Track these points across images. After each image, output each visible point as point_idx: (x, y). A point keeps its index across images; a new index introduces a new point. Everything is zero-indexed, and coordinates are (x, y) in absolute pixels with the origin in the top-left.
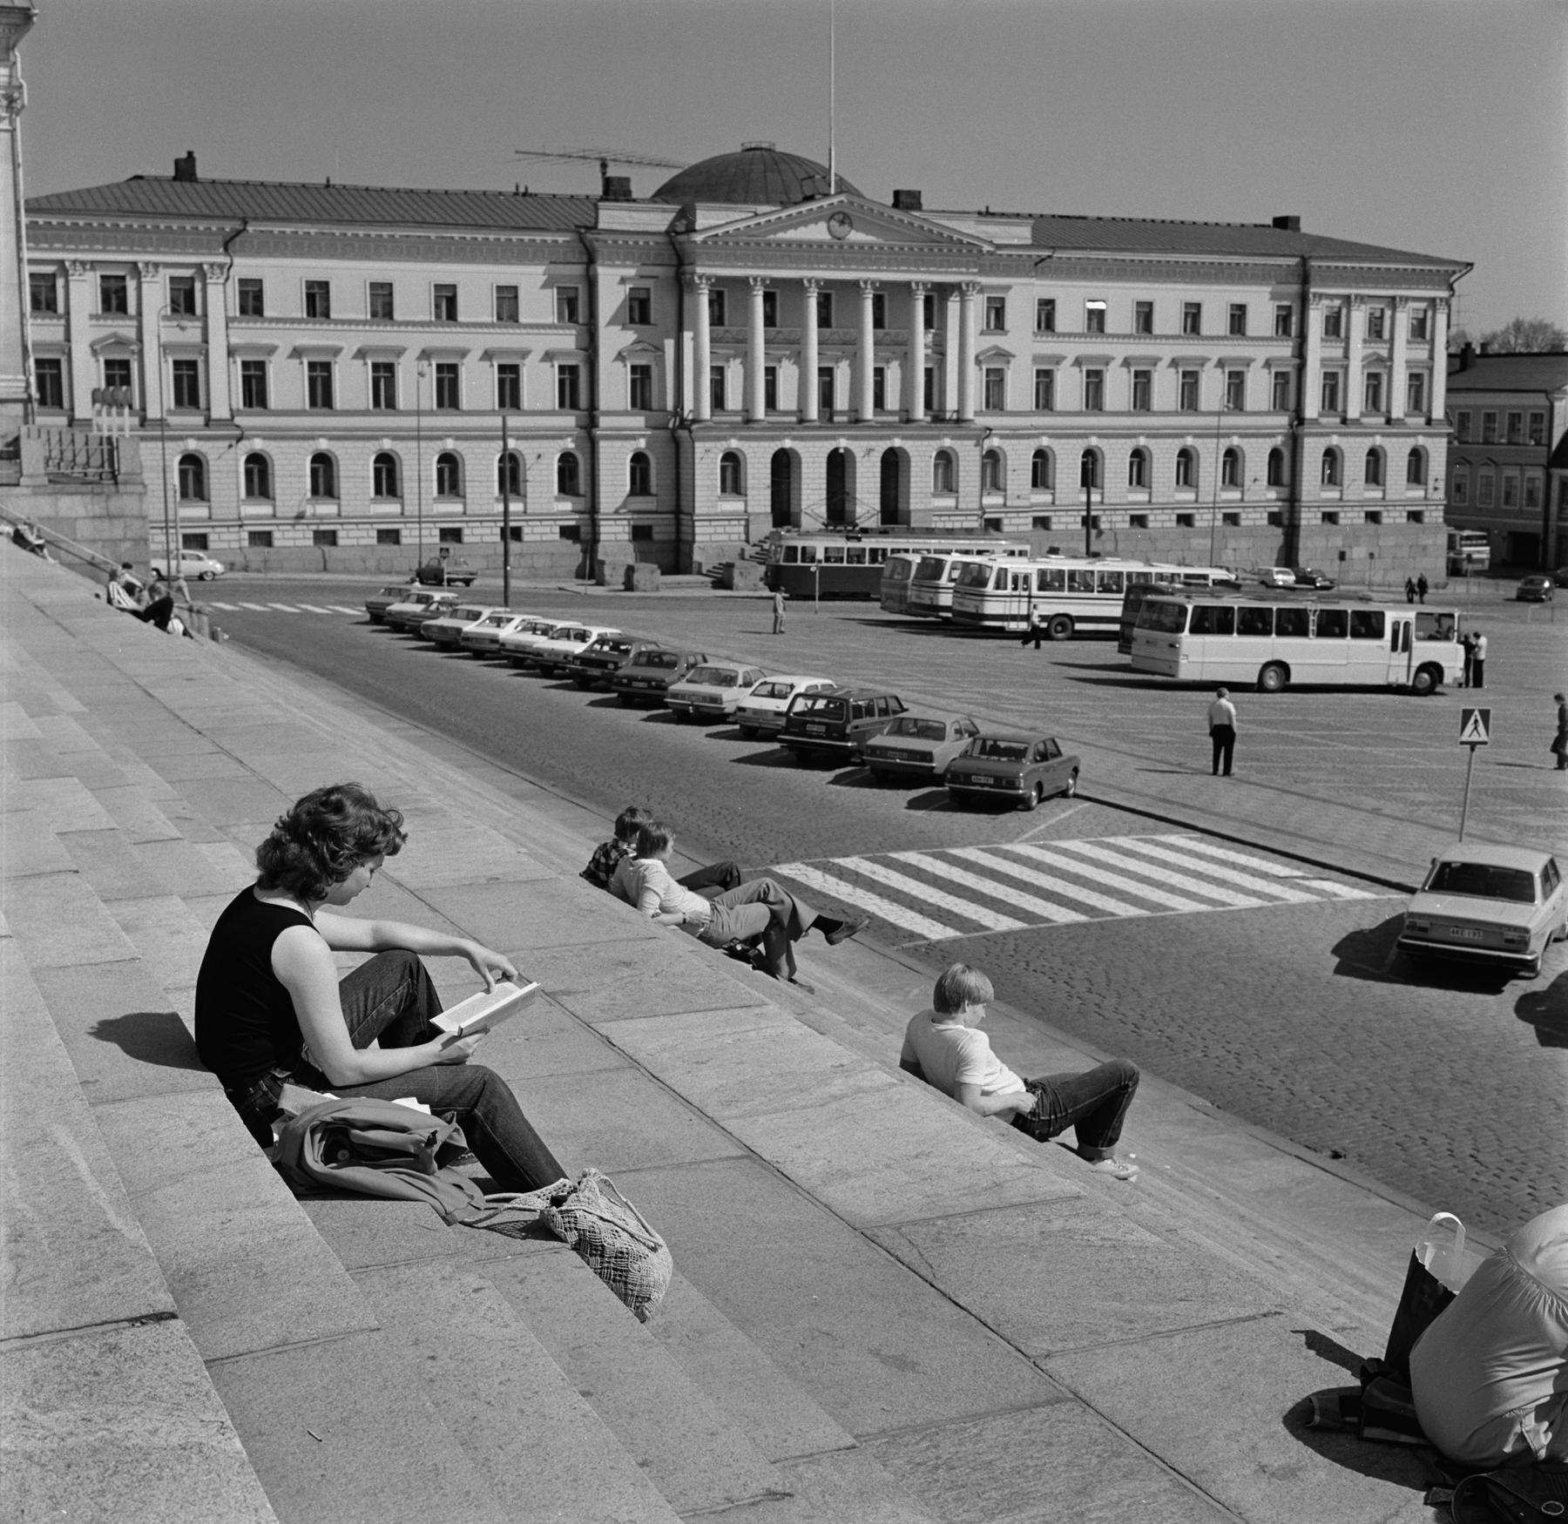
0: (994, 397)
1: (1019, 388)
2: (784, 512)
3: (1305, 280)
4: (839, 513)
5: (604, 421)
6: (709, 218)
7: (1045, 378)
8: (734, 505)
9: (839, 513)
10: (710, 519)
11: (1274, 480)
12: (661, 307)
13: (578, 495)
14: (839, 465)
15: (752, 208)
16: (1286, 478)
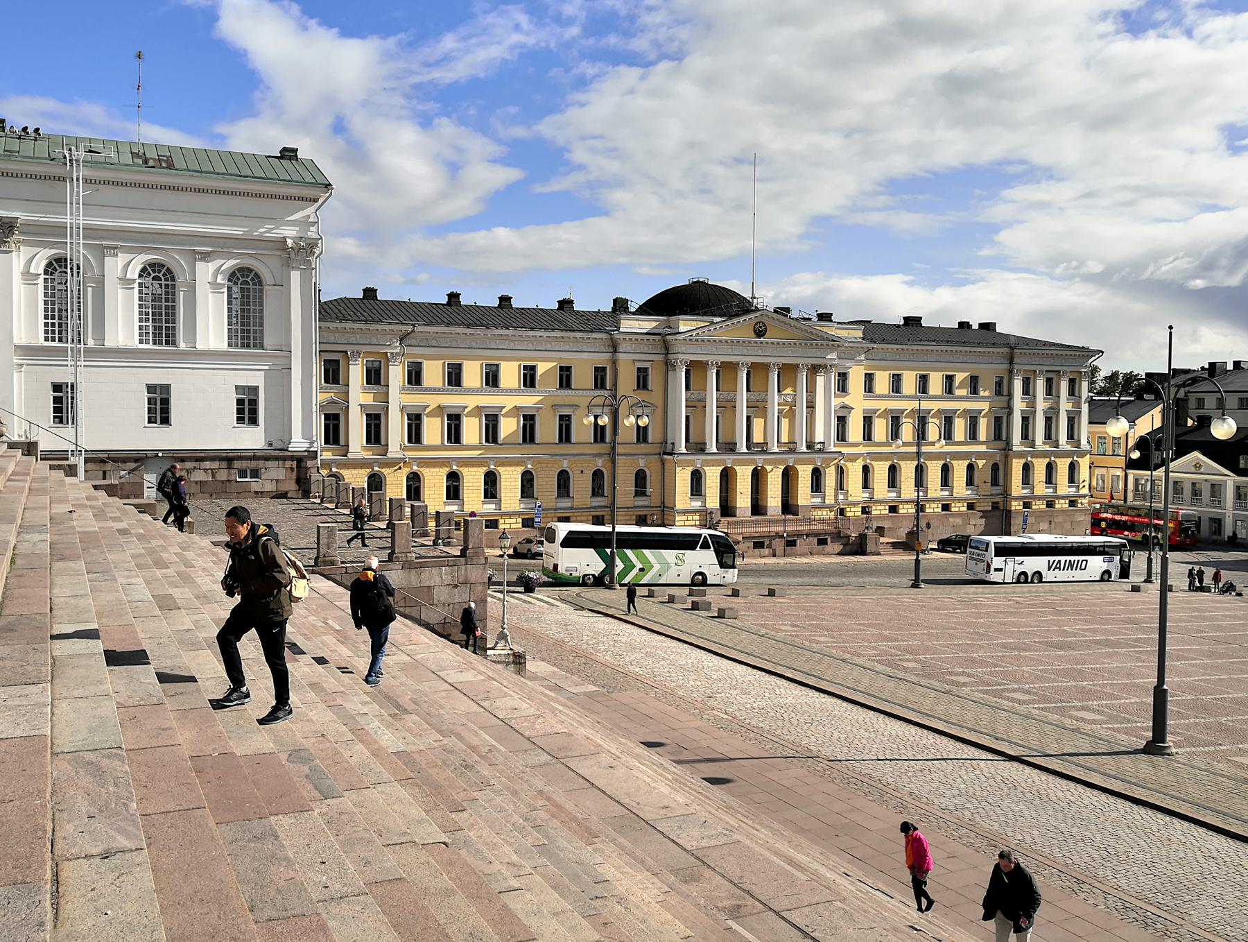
0: (842, 436)
1: (855, 430)
2: (727, 508)
3: (1011, 362)
4: (758, 508)
5: (619, 449)
6: (686, 324)
7: (868, 421)
8: (697, 504)
9: (758, 508)
10: (685, 512)
11: (995, 483)
12: (654, 380)
13: (603, 495)
14: (758, 478)
15: (710, 318)
16: (1001, 482)
